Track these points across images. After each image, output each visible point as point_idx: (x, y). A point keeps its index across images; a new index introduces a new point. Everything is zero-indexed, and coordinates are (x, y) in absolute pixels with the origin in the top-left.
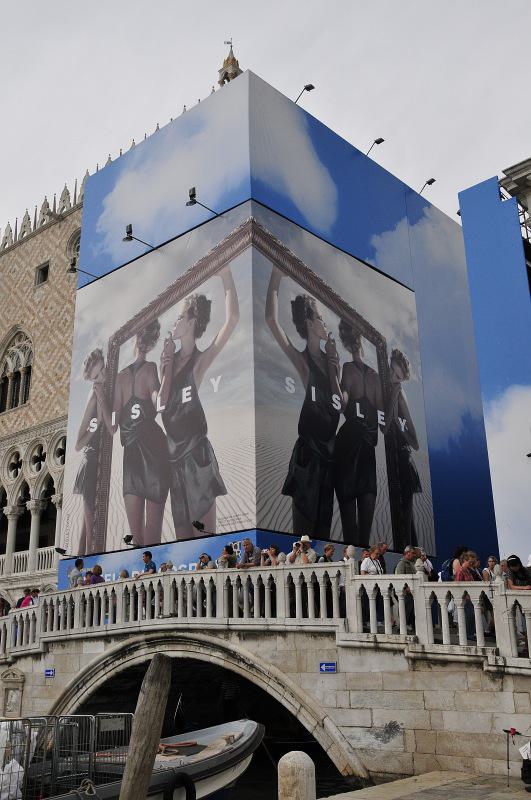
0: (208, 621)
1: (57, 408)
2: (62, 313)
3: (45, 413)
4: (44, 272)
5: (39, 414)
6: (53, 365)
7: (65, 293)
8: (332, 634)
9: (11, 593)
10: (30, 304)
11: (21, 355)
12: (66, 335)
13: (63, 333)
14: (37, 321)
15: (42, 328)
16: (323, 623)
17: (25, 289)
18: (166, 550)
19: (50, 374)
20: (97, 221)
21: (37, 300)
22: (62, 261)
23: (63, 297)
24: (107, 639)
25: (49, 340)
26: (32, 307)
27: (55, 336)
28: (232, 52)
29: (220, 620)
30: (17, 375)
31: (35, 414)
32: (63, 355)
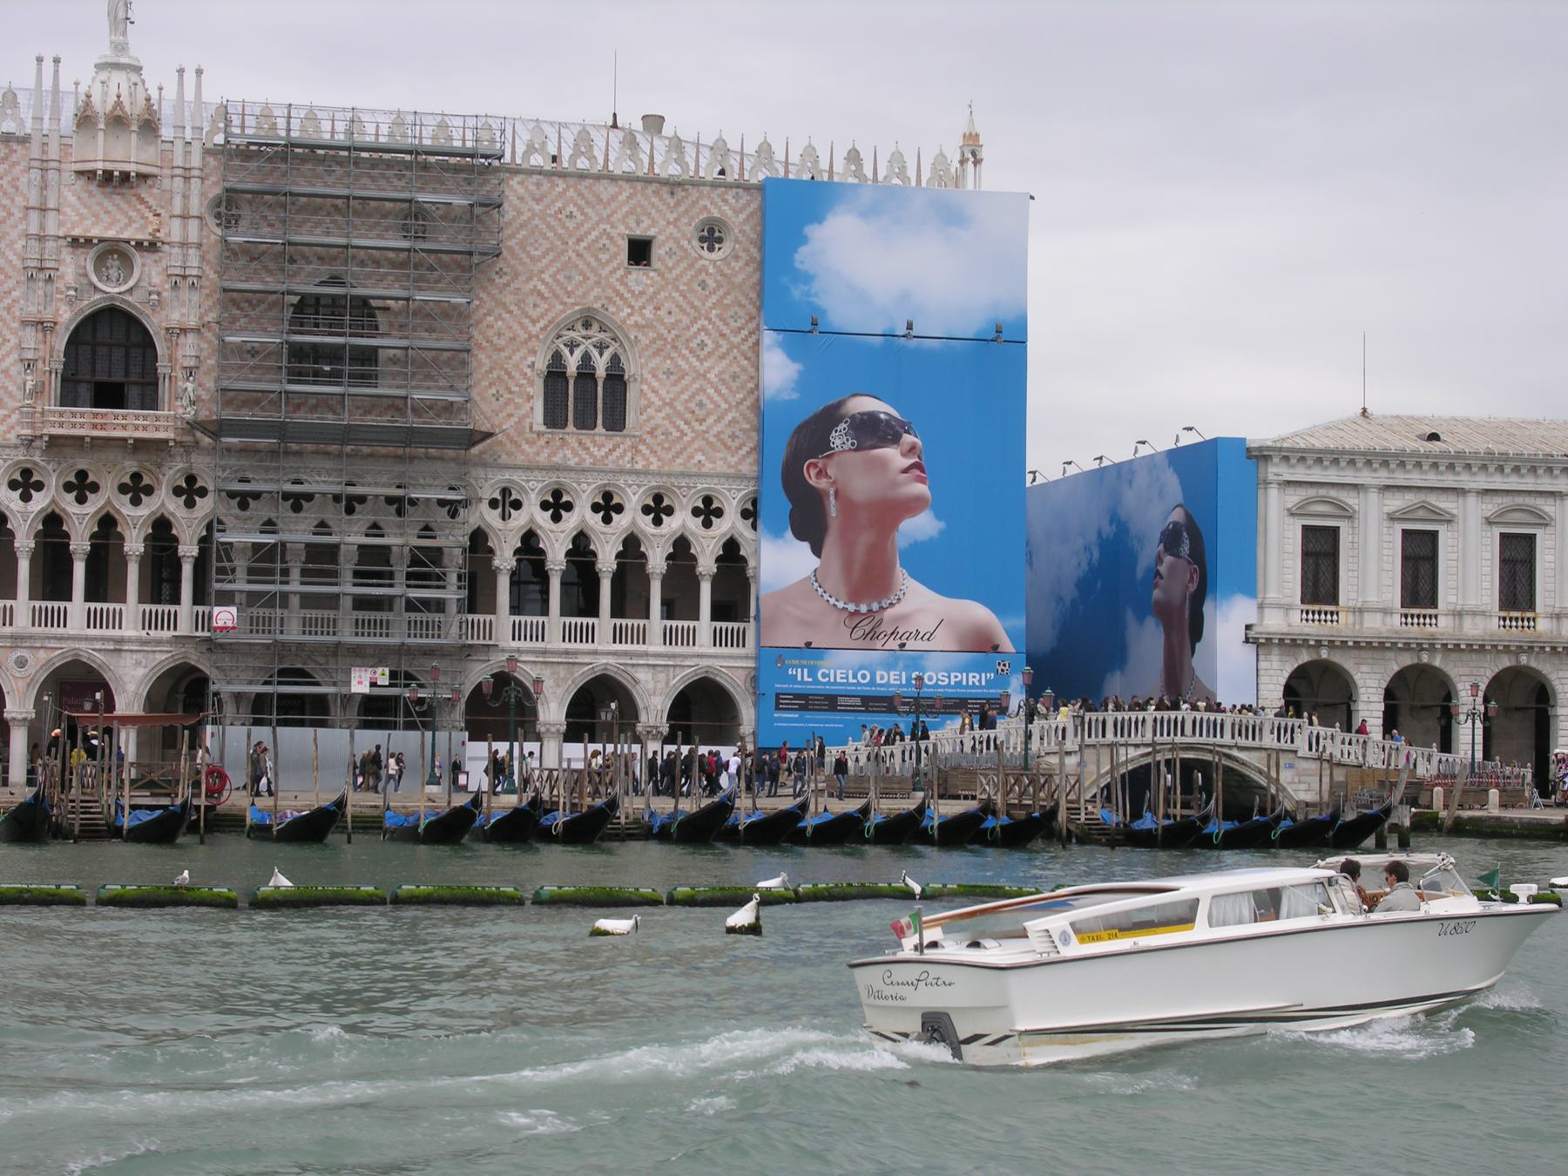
0: (1218, 740)
1: (700, 457)
2: (694, 329)
3: (677, 456)
4: (640, 251)
5: (661, 453)
6: (685, 396)
7: (697, 303)
8: (1296, 752)
9: (629, 669)
10: (622, 289)
11: (595, 353)
12: (706, 364)
13: (701, 361)
14: (636, 318)
15: (652, 335)
16: (1288, 746)
17: (604, 257)
18: (922, 657)
19: (680, 408)
20: (796, 252)
21: (637, 289)
22: (725, 276)
23: (693, 307)
24: (1137, 746)
25: (672, 359)
26: (627, 295)
27: (686, 360)
28: (972, 121)
29: (1227, 739)
30: (586, 374)
31: (654, 452)
32: (704, 391)
